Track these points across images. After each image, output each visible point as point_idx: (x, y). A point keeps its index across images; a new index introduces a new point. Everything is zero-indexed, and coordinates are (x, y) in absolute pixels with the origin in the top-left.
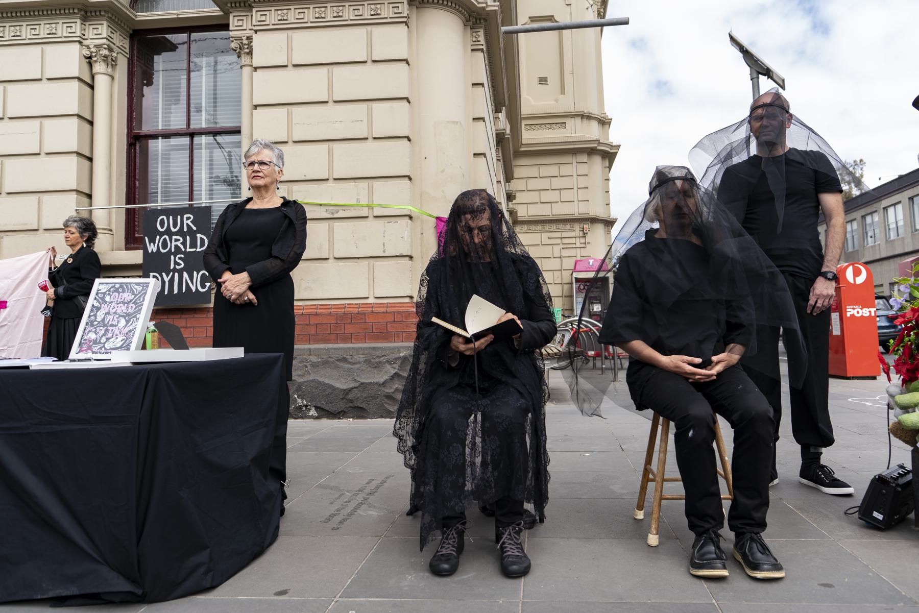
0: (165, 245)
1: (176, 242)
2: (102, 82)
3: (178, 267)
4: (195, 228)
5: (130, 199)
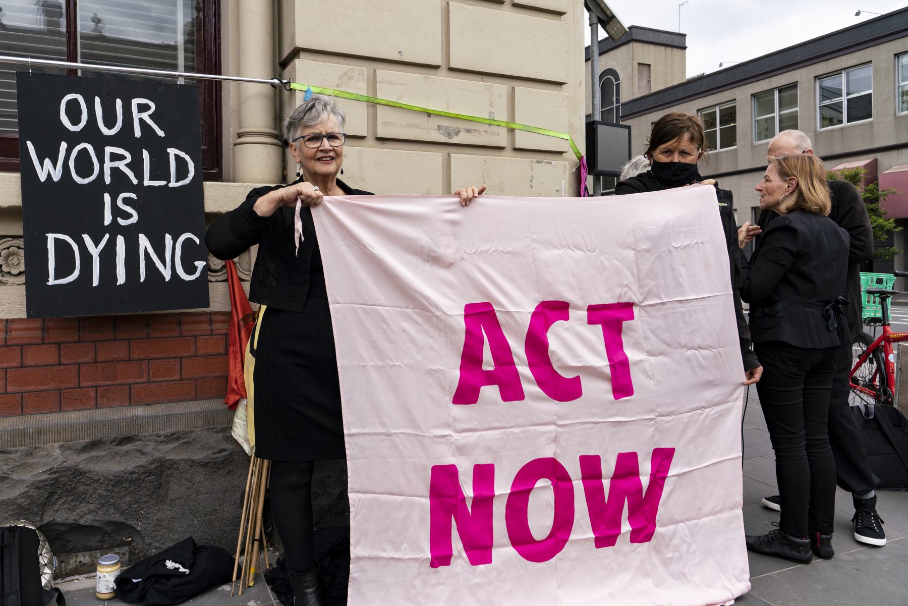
1: (114, 161)
3: (122, 222)
4: (161, 133)
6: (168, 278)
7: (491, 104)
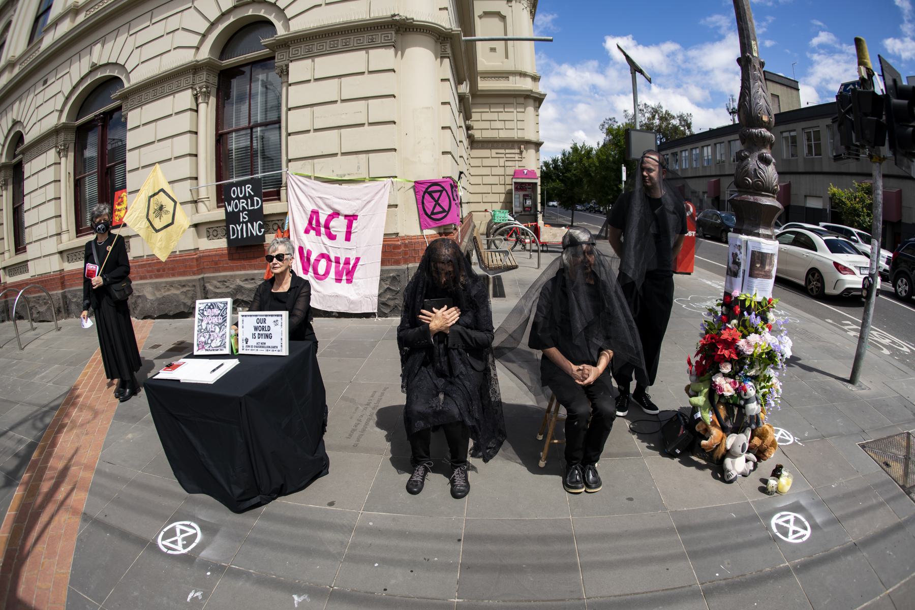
1: (242, 204)
2: (202, 107)
5: (219, 177)
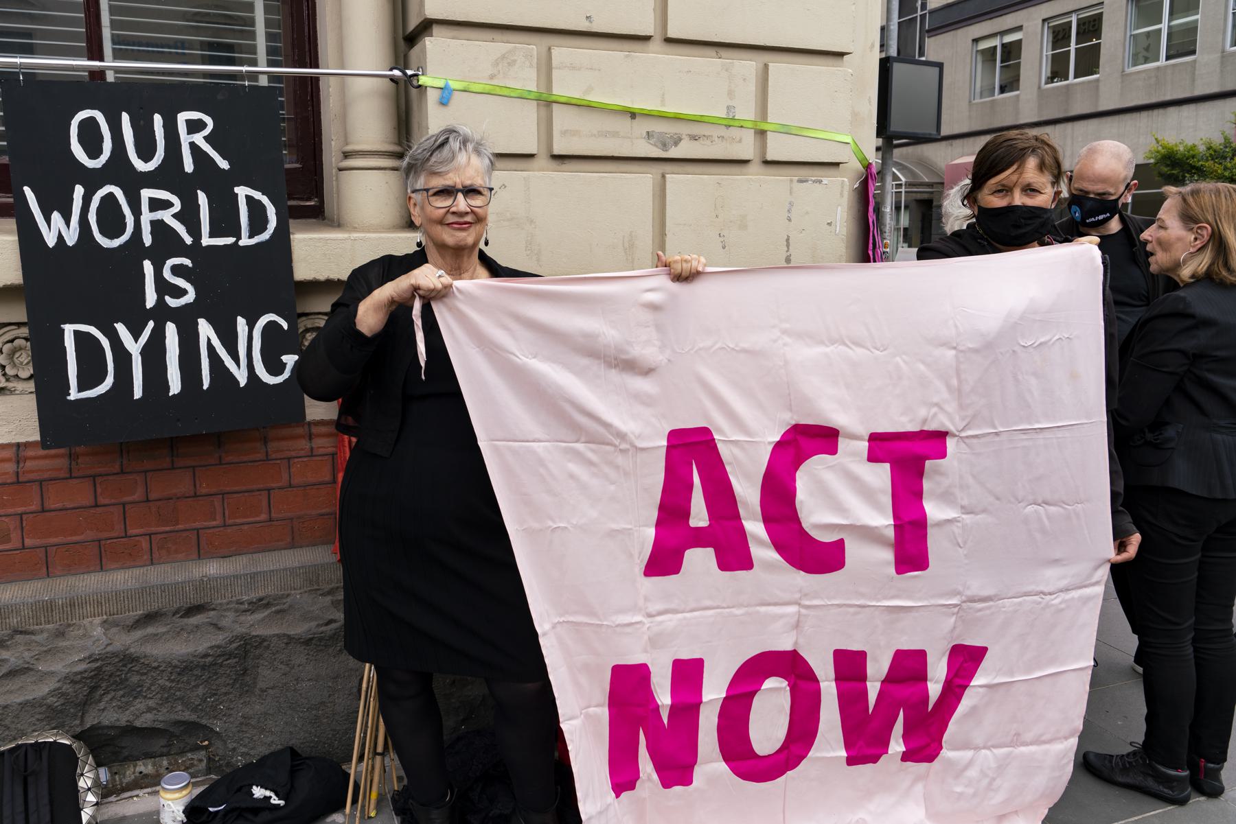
0: (111, 219)
1: (156, 210)
3: (172, 302)
4: (224, 164)
6: (243, 381)
7: (731, 94)
